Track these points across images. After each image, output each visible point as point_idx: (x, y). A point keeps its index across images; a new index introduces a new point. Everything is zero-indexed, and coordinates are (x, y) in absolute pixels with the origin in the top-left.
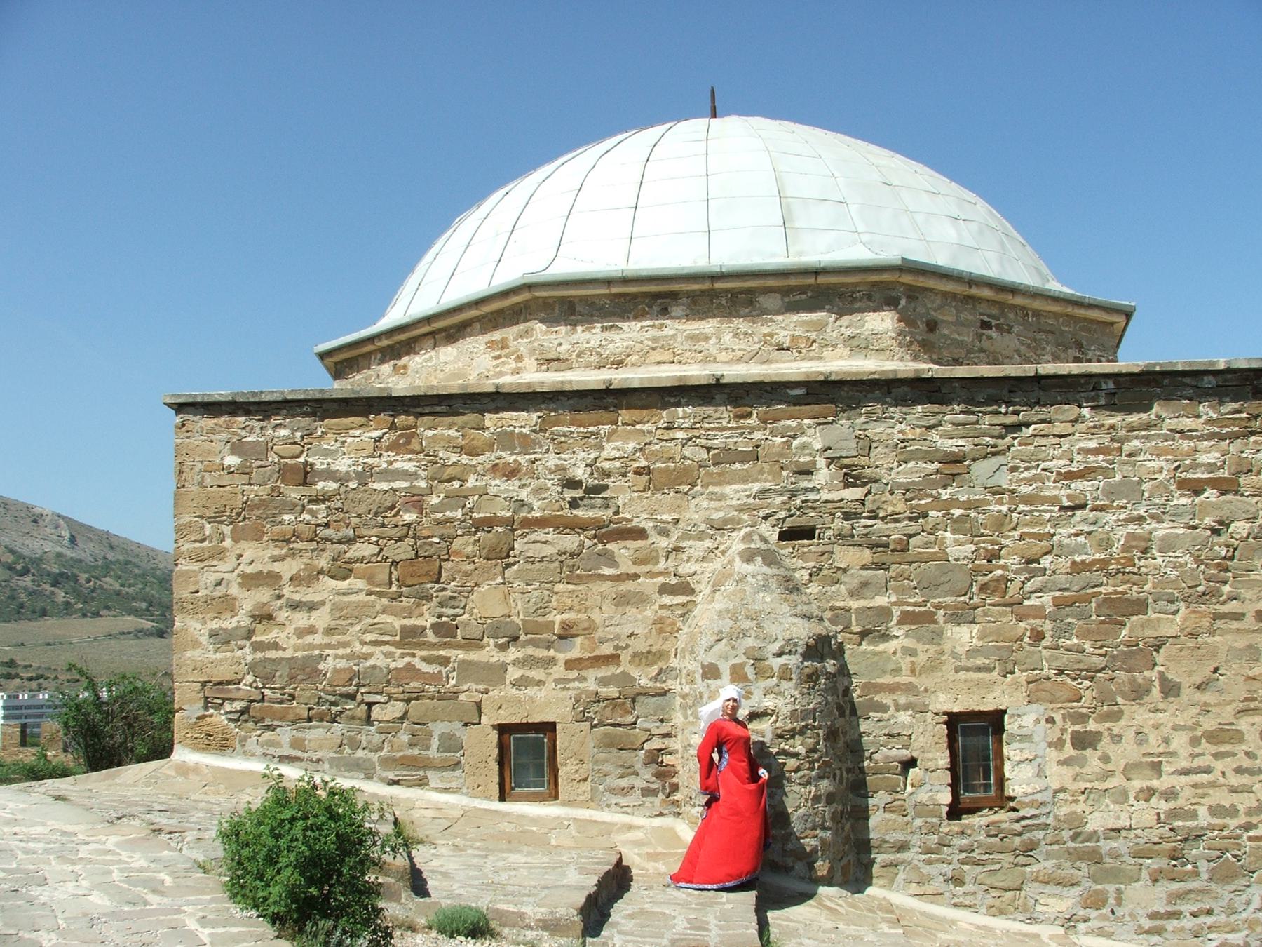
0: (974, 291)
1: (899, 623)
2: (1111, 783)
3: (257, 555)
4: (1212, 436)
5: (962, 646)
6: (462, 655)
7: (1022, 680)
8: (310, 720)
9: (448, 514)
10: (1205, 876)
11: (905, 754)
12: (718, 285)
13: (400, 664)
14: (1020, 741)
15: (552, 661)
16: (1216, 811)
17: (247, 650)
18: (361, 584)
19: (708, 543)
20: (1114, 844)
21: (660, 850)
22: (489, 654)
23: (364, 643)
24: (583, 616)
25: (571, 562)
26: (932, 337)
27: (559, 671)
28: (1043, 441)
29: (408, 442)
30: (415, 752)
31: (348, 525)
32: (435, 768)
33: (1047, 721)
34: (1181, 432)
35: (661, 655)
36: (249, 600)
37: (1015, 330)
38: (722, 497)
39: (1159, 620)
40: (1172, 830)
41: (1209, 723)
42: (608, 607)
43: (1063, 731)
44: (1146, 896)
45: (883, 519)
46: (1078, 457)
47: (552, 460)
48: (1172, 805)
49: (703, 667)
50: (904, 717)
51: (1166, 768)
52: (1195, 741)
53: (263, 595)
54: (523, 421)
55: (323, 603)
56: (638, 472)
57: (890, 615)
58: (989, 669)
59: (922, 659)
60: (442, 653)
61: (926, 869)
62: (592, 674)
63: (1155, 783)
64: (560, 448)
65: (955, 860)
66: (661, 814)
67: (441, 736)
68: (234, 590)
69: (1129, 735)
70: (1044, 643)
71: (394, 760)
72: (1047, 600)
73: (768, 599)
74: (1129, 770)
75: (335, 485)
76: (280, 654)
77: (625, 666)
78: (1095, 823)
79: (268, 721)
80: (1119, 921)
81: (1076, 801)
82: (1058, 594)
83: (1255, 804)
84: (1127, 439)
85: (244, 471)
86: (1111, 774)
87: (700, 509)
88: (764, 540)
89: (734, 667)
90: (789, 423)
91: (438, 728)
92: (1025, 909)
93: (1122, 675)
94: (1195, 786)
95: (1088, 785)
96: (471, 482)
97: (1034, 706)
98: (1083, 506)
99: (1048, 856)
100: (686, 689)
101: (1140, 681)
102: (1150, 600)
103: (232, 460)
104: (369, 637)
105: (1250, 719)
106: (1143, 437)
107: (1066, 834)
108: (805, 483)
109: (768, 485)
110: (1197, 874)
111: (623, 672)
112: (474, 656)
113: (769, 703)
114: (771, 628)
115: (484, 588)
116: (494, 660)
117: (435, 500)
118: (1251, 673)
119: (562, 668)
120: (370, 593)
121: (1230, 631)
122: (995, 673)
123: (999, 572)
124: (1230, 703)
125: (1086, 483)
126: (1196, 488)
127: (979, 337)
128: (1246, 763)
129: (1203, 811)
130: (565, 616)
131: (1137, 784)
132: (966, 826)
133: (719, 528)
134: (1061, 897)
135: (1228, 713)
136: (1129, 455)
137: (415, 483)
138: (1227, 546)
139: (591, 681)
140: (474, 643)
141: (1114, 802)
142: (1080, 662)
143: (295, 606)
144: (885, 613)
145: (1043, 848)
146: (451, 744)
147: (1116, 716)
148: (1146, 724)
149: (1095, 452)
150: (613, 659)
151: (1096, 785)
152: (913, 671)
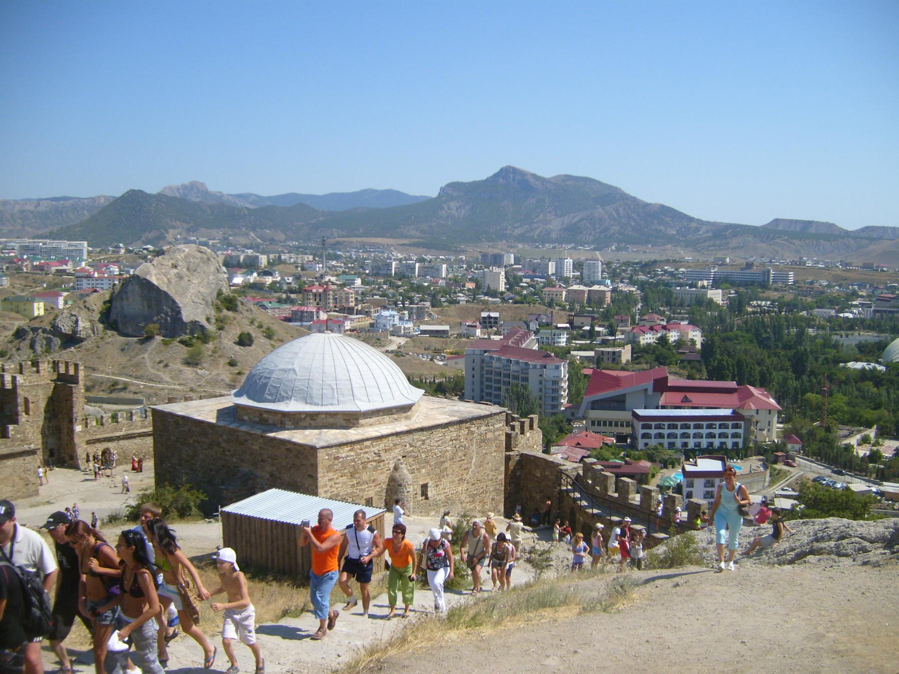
3: (331, 475)
22: (364, 487)
36: (330, 484)
47: (373, 449)
54: (368, 443)
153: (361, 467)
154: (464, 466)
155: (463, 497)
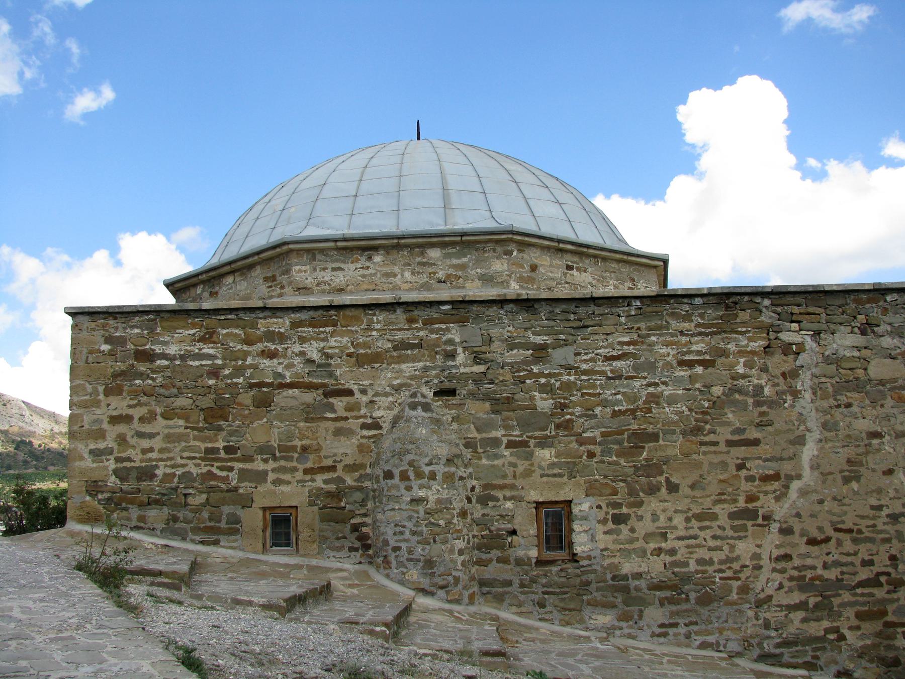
0: (561, 245)
1: (506, 447)
2: (637, 545)
3: (119, 405)
4: (700, 334)
5: (545, 461)
6: (240, 465)
7: (582, 482)
8: (149, 504)
9: (234, 380)
10: (693, 601)
11: (509, 526)
12: (403, 241)
13: (204, 470)
14: (581, 520)
15: (295, 469)
16: (700, 562)
17: (112, 461)
18: (181, 422)
19: (390, 399)
20: (637, 582)
21: (356, 582)
23: (182, 458)
24: (315, 443)
25: (308, 410)
26: (533, 274)
27: (299, 475)
28: (596, 337)
29: (211, 337)
30: (212, 524)
31: (174, 387)
32: (225, 534)
33: (597, 507)
34: (681, 332)
35: (362, 466)
36: (112, 431)
37: (590, 270)
38: (400, 371)
39: (666, 446)
40: (673, 573)
41: (697, 510)
42: (330, 436)
43: (607, 513)
44: (655, 615)
45: (496, 384)
46: (618, 347)
47: (297, 348)
48: (674, 558)
49: (384, 472)
50: (509, 505)
51: (669, 536)
52: (688, 520)
53: (121, 428)
55: (158, 434)
56: (349, 355)
57: (501, 442)
58: (560, 475)
59: (520, 469)
60: (229, 464)
61: (522, 597)
62: (320, 478)
63: (663, 545)
64: (302, 340)
65: (540, 592)
66: (360, 563)
67: (228, 515)
68: (105, 426)
69: (648, 517)
70: (594, 459)
71: (200, 528)
72: (597, 433)
73: (424, 432)
74: (648, 537)
75: (167, 363)
76: (133, 464)
77: (339, 472)
78: (627, 568)
79: (124, 505)
80: (640, 629)
81: (615, 556)
82: (603, 430)
83: (724, 557)
84: (649, 336)
85: (112, 354)
86: (637, 539)
87: (386, 377)
88: (424, 396)
89: (401, 472)
90: (441, 326)
91: (226, 510)
92: (581, 621)
93: (643, 479)
94: (687, 547)
95: (622, 546)
96: (249, 361)
97: (588, 498)
98: (620, 377)
99: (598, 589)
100: (375, 487)
101: (654, 482)
102: (661, 435)
103: (106, 347)
104: (185, 454)
105: (722, 506)
106: (657, 334)
107: (609, 576)
108: (450, 363)
109: (428, 364)
110: (687, 600)
111: (338, 477)
112: (248, 466)
113: (422, 493)
114: (425, 449)
115: (255, 425)
116: (261, 469)
117: (227, 372)
118: (722, 477)
119: (301, 474)
120: (186, 428)
121: (710, 452)
122: (565, 479)
123: (568, 417)
124: (709, 496)
125: (622, 363)
126: (690, 364)
127: (565, 274)
128: (719, 532)
129: (692, 562)
130: (304, 442)
131: (652, 545)
132: (547, 571)
133: (397, 389)
134: (605, 615)
135: (708, 502)
136: (650, 345)
137: (216, 362)
138: (709, 401)
139: (319, 480)
140: (248, 459)
141: (638, 557)
142: (618, 471)
143: (141, 435)
144: (496, 442)
145: (594, 586)
146: (235, 520)
147: (640, 504)
148: (658, 510)
149: (628, 344)
150: (333, 468)
151: (627, 546)
152: (515, 476)
153: (246, 398)
154: (756, 468)
155: (767, 581)
